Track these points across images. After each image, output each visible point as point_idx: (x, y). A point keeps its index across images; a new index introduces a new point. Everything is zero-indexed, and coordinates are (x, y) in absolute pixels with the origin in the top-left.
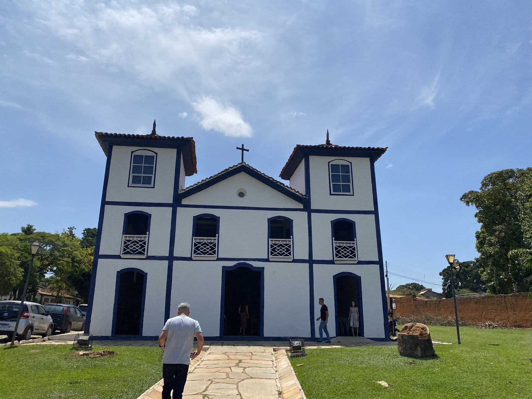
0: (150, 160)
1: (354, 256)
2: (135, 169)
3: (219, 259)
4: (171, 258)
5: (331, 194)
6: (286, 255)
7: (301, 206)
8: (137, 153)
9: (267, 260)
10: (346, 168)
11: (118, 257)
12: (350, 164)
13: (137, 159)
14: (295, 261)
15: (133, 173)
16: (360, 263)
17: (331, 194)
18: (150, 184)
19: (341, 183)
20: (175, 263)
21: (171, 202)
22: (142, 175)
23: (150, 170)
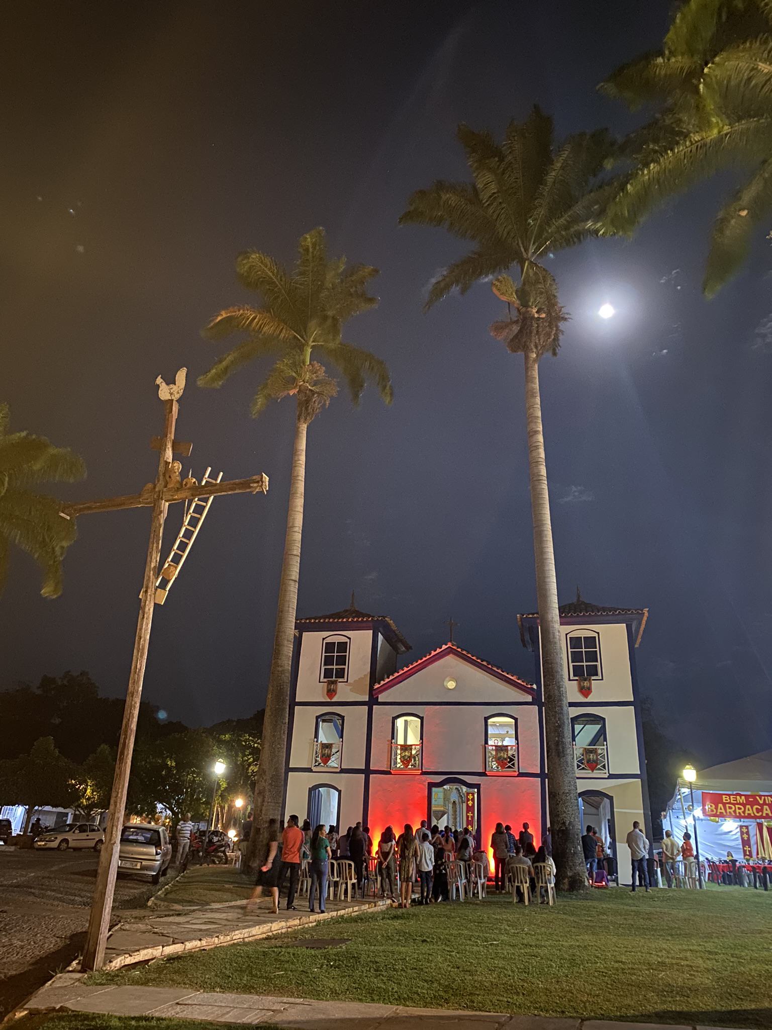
0: (343, 647)
1: (604, 766)
2: (328, 661)
3: (423, 773)
4: (367, 771)
5: (570, 680)
6: (509, 767)
7: (529, 698)
8: (329, 640)
9: (483, 774)
10: (591, 642)
11: (309, 770)
12: (596, 635)
13: (329, 647)
14: (521, 775)
15: (325, 665)
16: (611, 776)
17: (570, 680)
18: (343, 677)
19: (585, 664)
20: (372, 777)
21: (366, 698)
22: (335, 667)
23: (342, 660)
